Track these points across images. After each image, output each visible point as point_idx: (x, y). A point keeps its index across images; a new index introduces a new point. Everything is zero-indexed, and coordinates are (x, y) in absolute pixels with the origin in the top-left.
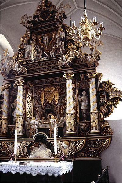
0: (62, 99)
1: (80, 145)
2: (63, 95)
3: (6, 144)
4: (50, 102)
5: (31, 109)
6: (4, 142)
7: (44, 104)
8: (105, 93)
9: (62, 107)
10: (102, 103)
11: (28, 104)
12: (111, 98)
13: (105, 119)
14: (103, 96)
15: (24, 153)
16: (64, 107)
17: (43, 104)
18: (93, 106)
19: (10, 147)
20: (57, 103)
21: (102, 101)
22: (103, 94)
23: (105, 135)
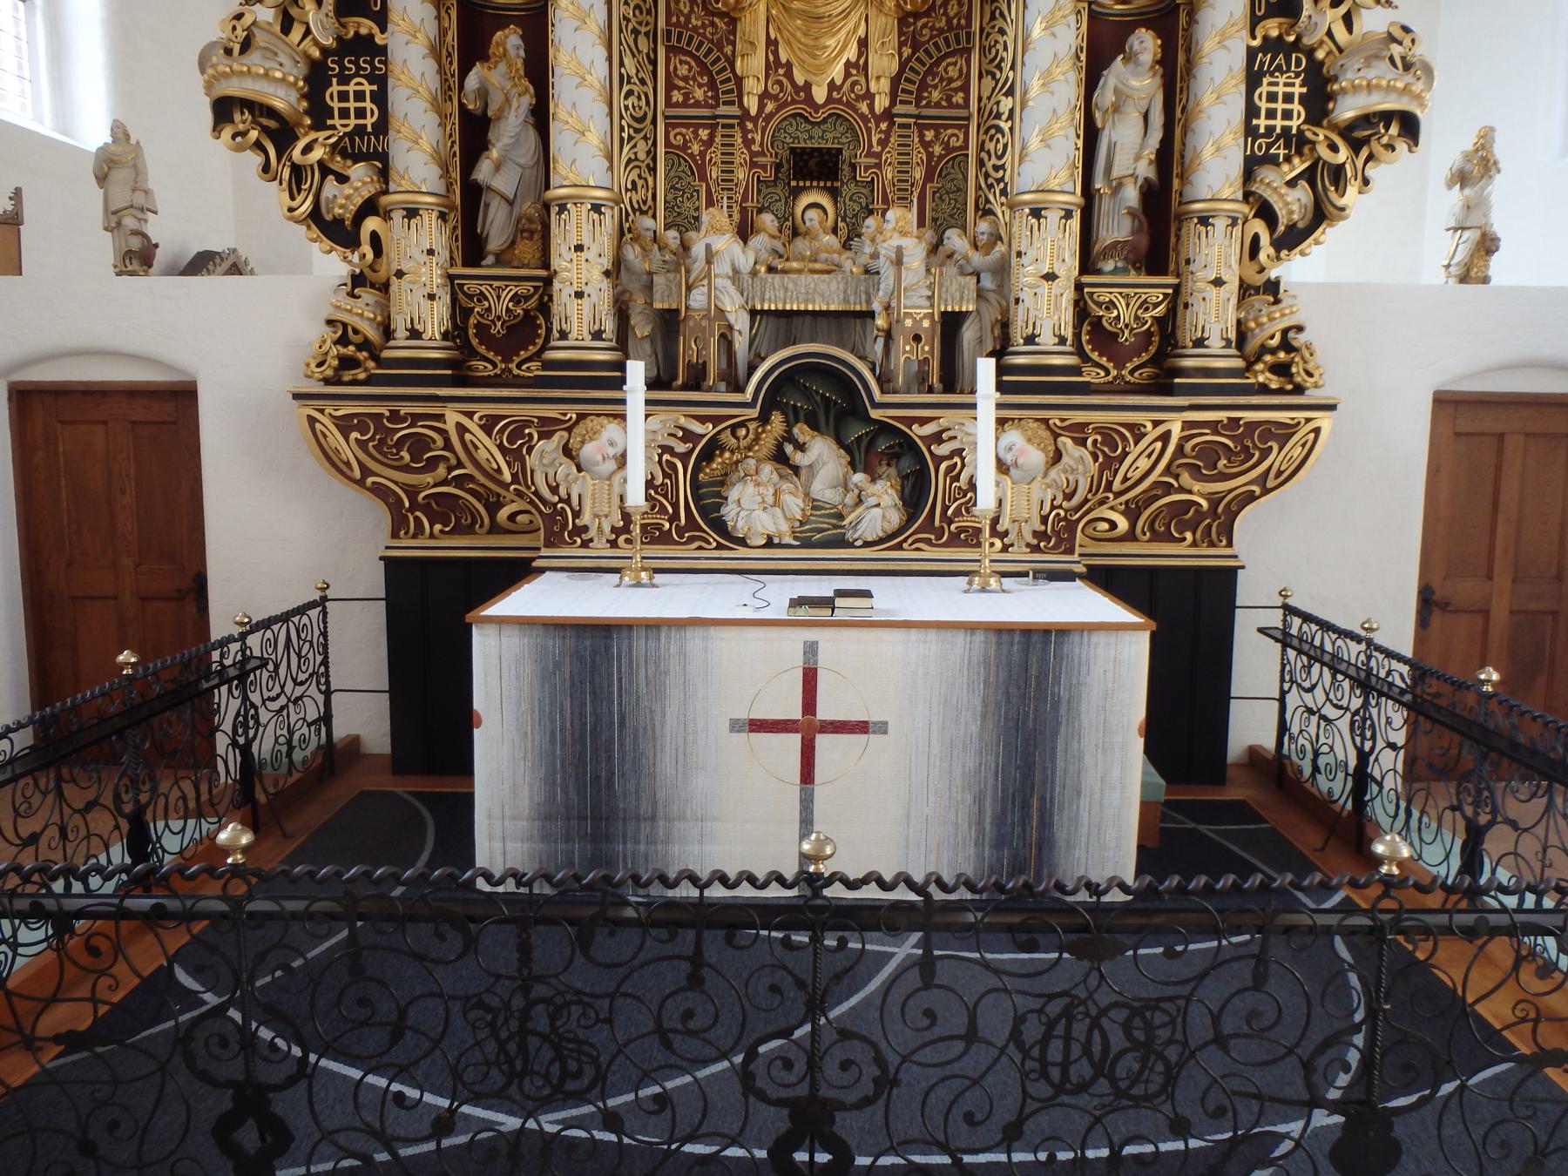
0: (927, 73)
2: (941, 43)
3: (487, 429)
4: (820, 95)
5: (645, 138)
6: (470, 415)
7: (761, 106)
8: (1298, 64)
9: (926, 145)
10: (1269, 146)
11: (625, 89)
12: (1346, 110)
13: (1295, 270)
14: (1281, 90)
15: (663, 510)
16: (937, 150)
17: (752, 104)
19: (531, 461)
20: (881, 103)
21: (1269, 130)
22: (1279, 68)
23: (1264, 389)
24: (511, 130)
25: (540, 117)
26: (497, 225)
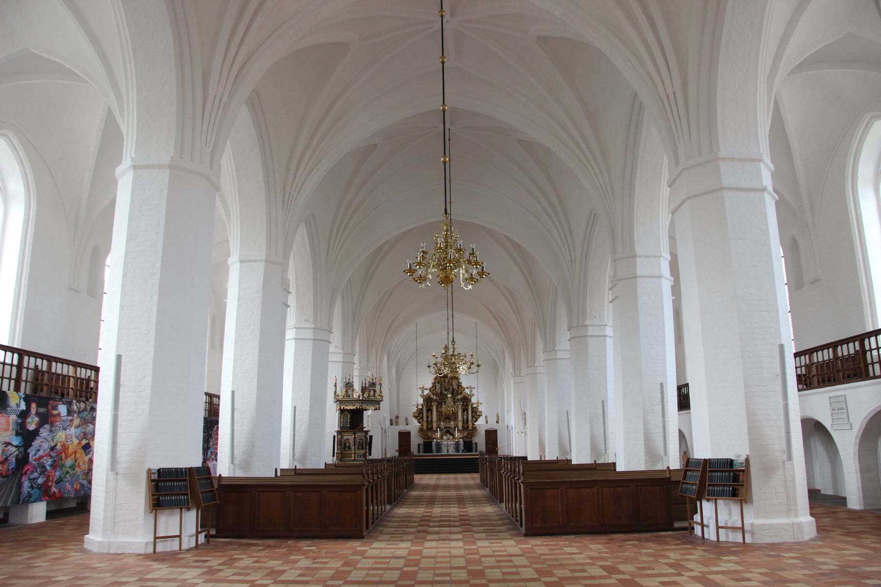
1: (465, 434)
12: (478, 414)
13: (475, 423)
18: (470, 418)
24: (430, 417)
25: (432, 416)
26: (429, 422)
